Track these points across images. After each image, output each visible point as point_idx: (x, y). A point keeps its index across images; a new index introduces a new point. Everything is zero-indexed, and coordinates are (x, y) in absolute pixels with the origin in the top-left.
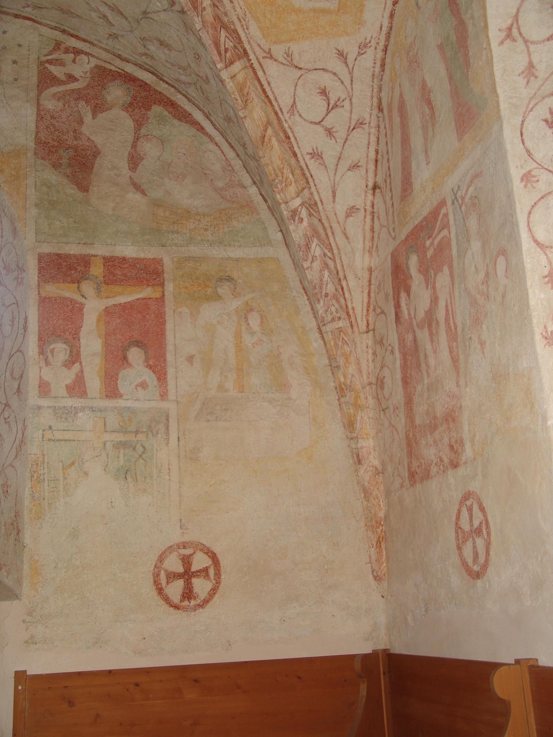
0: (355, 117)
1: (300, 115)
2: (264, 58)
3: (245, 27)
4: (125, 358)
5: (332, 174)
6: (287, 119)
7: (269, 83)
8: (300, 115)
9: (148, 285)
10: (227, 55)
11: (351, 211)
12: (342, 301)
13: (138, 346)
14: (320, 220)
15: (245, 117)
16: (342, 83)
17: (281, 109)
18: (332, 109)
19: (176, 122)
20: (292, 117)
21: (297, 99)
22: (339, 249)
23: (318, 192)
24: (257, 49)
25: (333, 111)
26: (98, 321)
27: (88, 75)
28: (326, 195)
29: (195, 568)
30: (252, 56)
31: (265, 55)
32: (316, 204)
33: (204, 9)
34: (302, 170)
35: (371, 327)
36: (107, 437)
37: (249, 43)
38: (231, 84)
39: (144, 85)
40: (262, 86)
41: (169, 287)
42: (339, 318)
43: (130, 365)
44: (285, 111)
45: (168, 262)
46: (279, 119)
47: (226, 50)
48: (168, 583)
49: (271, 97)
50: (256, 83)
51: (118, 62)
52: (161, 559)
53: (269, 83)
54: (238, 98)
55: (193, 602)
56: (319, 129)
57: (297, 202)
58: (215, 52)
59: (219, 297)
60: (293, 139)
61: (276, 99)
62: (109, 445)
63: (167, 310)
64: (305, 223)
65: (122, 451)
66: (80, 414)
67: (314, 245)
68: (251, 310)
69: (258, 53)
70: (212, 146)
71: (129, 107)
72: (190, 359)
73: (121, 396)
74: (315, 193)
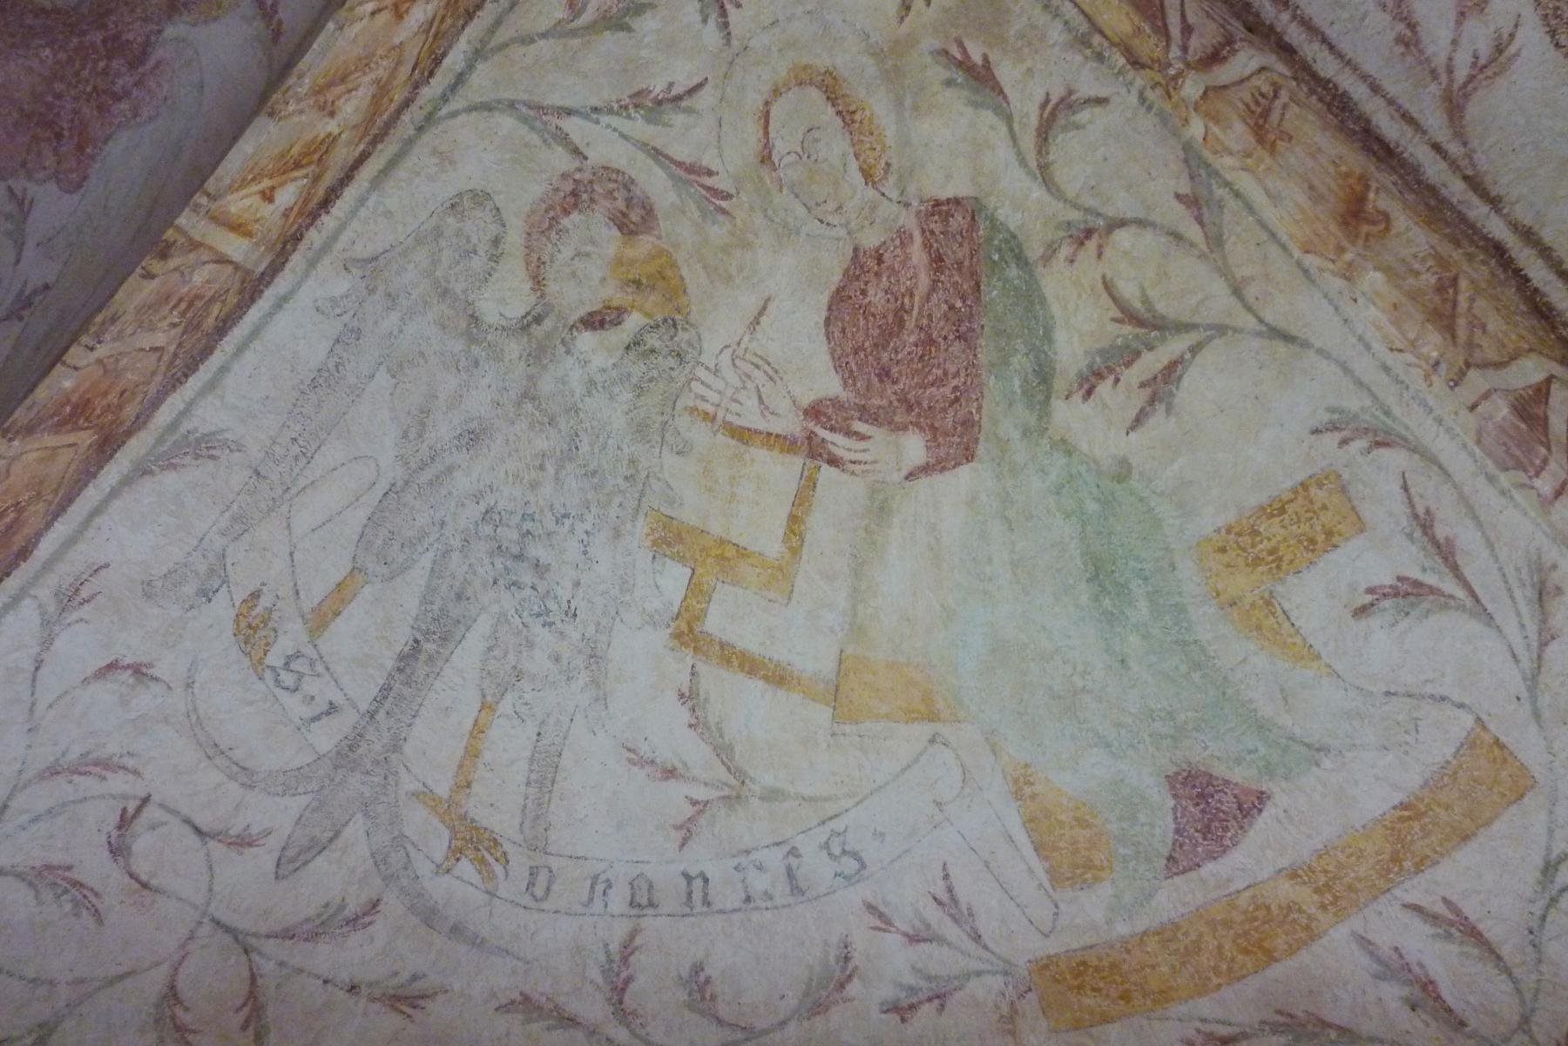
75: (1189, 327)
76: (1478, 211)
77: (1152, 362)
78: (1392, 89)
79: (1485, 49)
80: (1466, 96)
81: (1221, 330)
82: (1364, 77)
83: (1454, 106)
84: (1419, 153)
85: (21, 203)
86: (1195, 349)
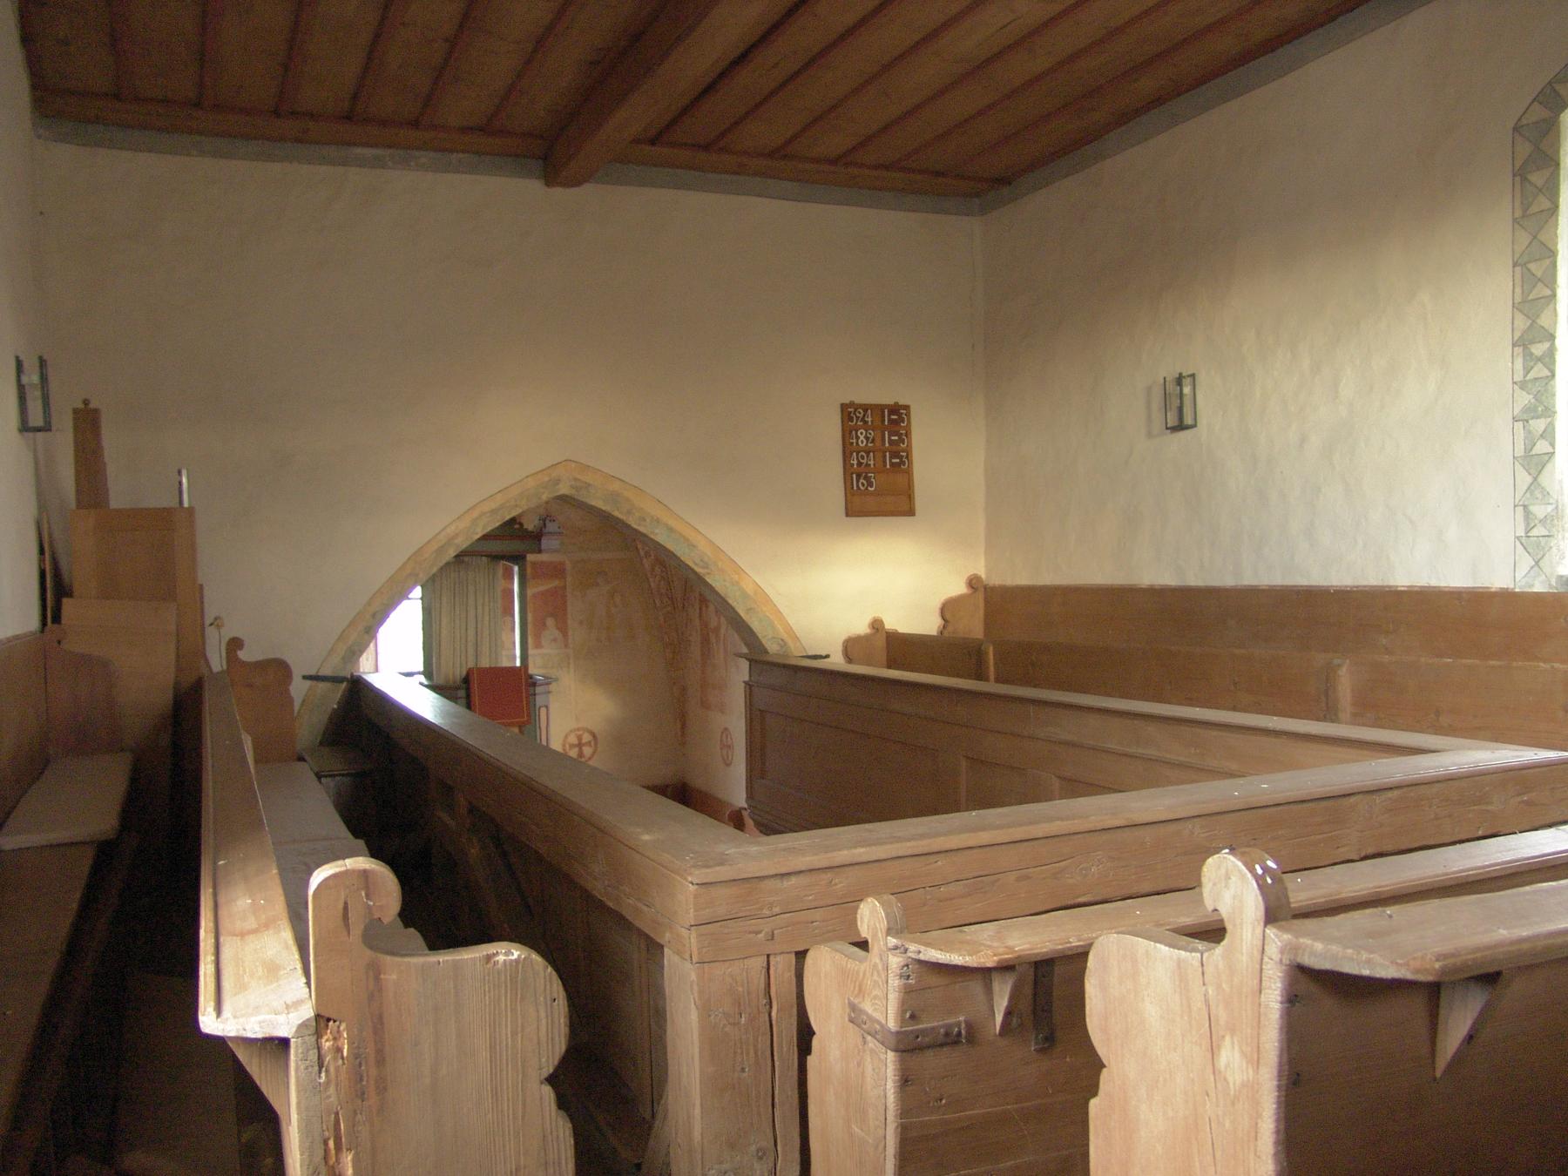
29: (584, 741)
41: (569, 579)
45: (569, 566)
52: (566, 737)
59: (598, 584)
67: (657, 568)
72: (581, 623)
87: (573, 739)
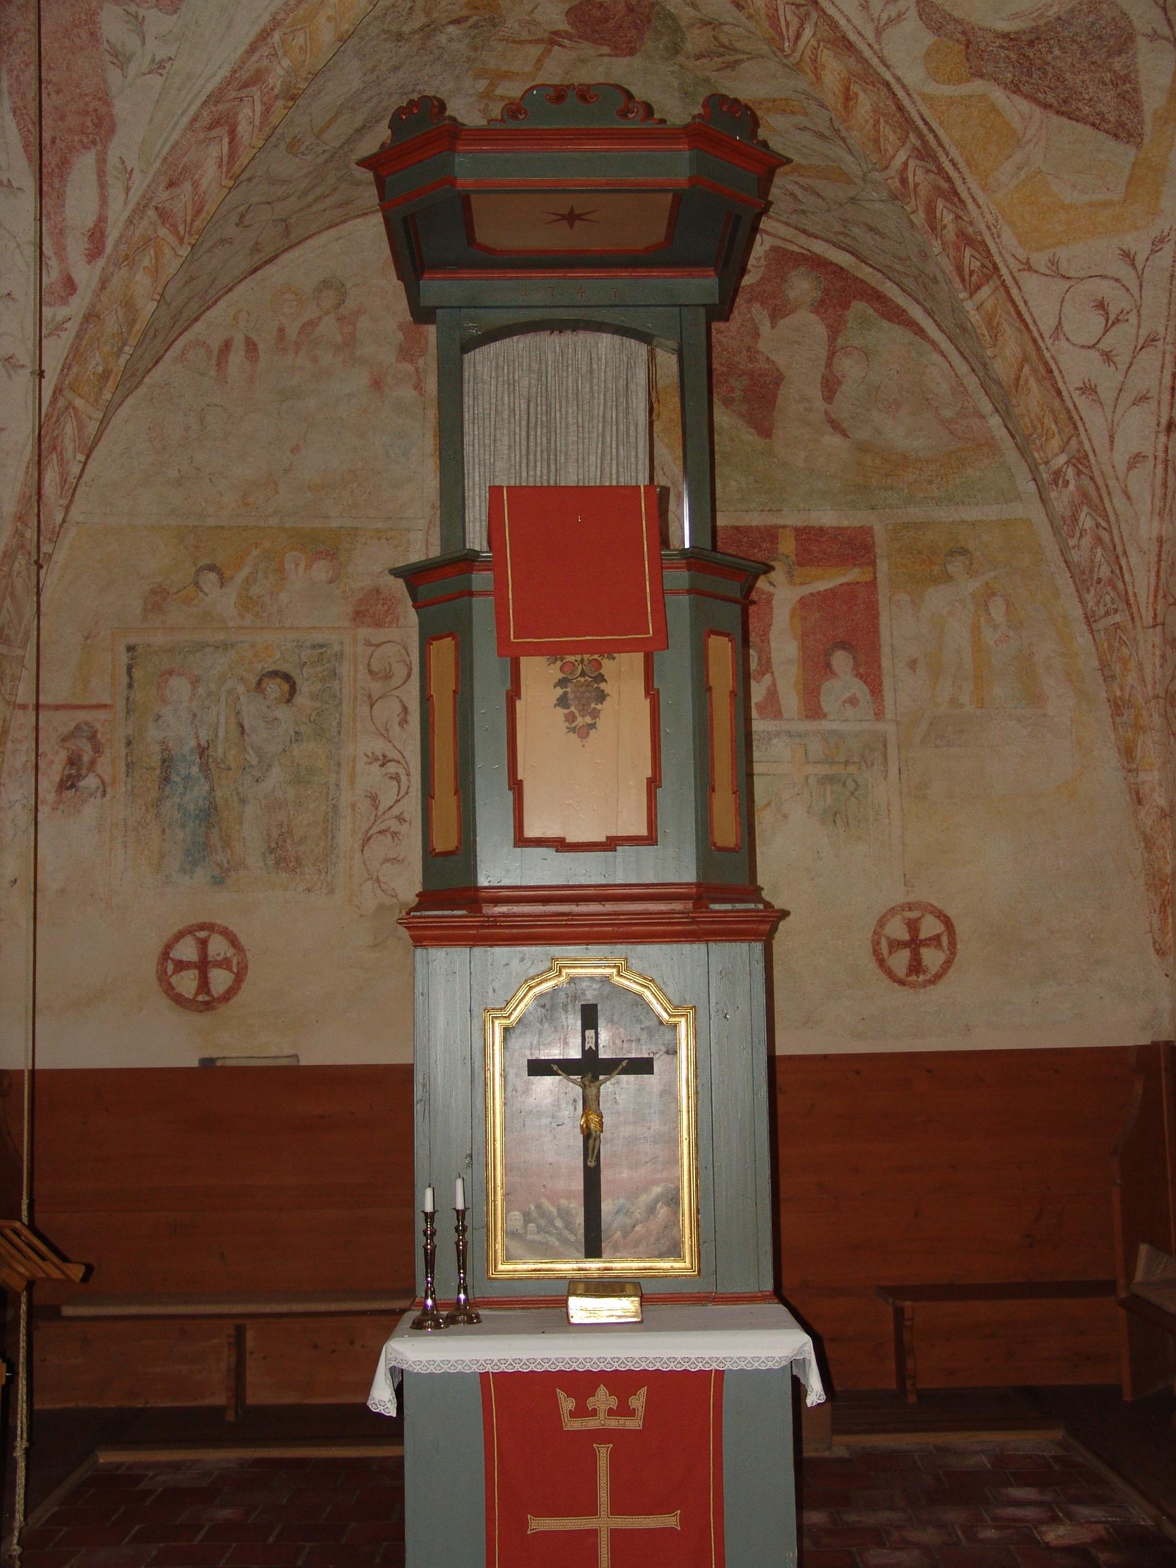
0: (1144, 332)
1: (1067, 339)
2: (1019, 270)
3: (996, 236)
4: (828, 665)
5: (1109, 411)
6: (1049, 346)
7: (1026, 303)
8: (1067, 339)
9: (854, 565)
10: (973, 278)
11: (1136, 460)
12: (1120, 585)
13: (844, 649)
14: (1092, 478)
15: (995, 357)
16: (1128, 290)
17: (1041, 335)
18: (1113, 324)
19: (885, 324)
20: (1056, 343)
21: (1063, 318)
22: (1116, 515)
23: (1090, 440)
24: (1011, 260)
25: (1114, 328)
26: (792, 616)
27: (763, 262)
28: (1101, 442)
29: (923, 935)
30: (1004, 271)
31: (1022, 267)
32: (1086, 456)
33: (944, 227)
34: (1068, 411)
35: (1159, 620)
36: (809, 769)
37: (1001, 253)
38: (977, 317)
39: (838, 271)
40: (1016, 307)
41: (883, 566)
42: (1116, 611)
43: (835, 674)
44: (1046, 335)
45: (880, 534)
46: (1038, 348)
47: (971, 273)
48: (890, 953)
49: (1029, 320)
50: (1009, 305)
51: (802, 239)
52: (882, 923)
53: (1026, 303)
54: (986, 334)
55: (922, 978)
56: (1094, 354)
57: (1062, 459)
58: (958, 279)
59: (948, 578)
60: (1056, 373)
61: (1035, 322)
62: (811, 780)
63: (880, 598)
64: (1071, 487)
65: (828, 787)
66: (775, 741)
67: (1083, 515)
68: (994, 594)
69: (1011, 266)
70: (936, 357)
71: (820, 307)
72: (913, 664)
73: (825, 716)
74: (1086, 442)
75: (747, 53)
76: (882, 69)
77: (728, 58)
78: (856, 22)
79: (894, 14)
80: (884, 30)
81: (762, 57)
82: (845, 16)
83: (878, 32)
84: (861, 46)
85: (136, 17)
86: (748, 59)
87: (897, 930)
